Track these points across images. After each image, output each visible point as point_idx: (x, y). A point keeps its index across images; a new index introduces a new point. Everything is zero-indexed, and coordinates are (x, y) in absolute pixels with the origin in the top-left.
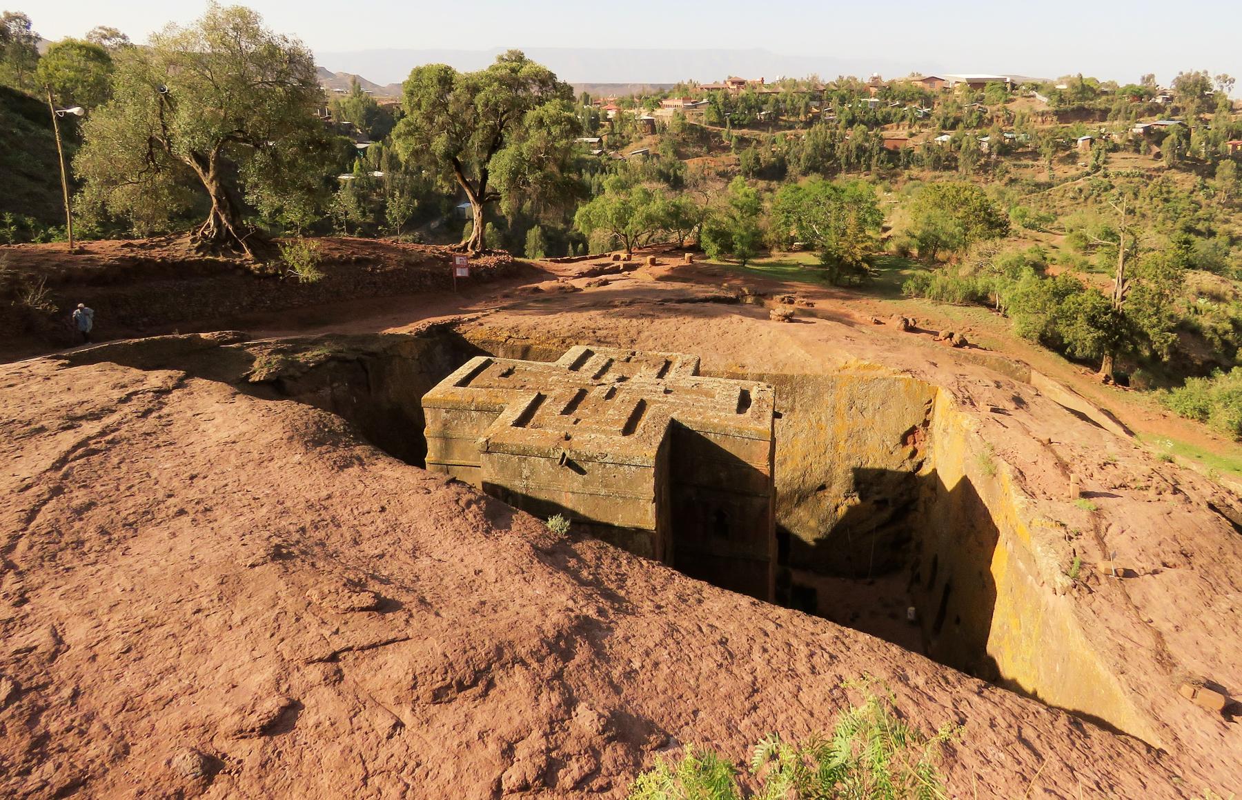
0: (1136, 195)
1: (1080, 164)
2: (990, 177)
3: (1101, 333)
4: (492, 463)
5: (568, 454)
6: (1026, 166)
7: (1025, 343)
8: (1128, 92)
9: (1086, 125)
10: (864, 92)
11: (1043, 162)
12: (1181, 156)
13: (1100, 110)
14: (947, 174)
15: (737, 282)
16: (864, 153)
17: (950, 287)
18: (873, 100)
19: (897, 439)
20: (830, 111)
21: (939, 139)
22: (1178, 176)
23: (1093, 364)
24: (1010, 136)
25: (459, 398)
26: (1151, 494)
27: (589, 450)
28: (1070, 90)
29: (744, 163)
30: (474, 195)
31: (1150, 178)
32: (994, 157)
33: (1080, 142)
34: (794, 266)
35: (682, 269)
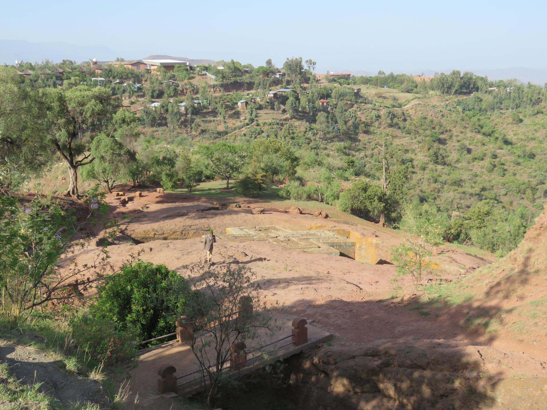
1: (242, 118)
2: (189, 130)
6: (210, 121)
8: (261, 71)
9: (240, 93)
11: (220, 118)
13: (247, 83)
18: (100, 79)
21: (153, 105)
22: (297, 123)
31: (282, 125)
32: (189, 116)
33: (239, 104)
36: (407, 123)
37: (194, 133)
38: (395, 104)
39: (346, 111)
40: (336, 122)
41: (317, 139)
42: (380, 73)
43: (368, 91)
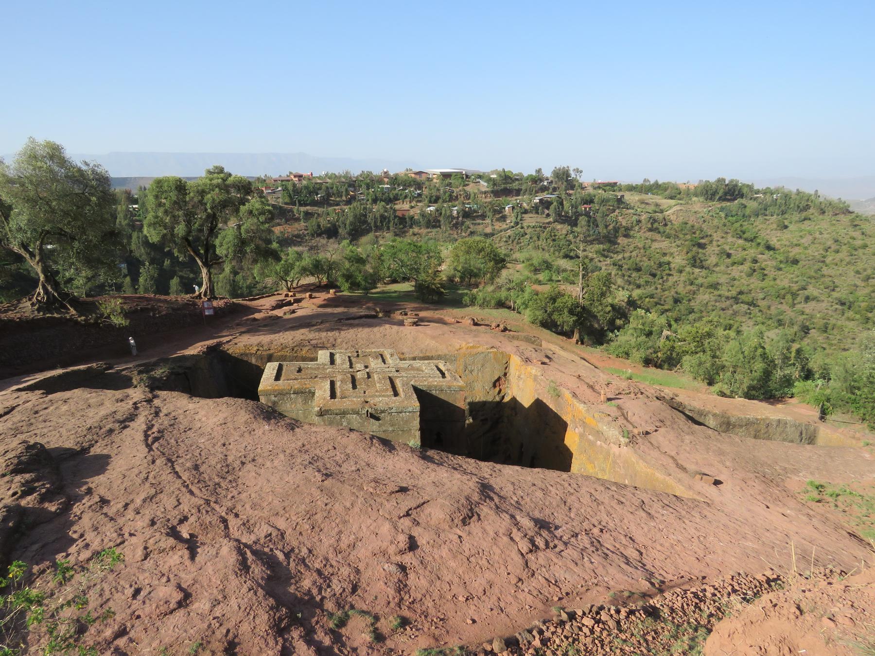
0: (538, 238)
1: (508, 221)
3: (575, 318)
4: (324, 421)
5: (370, 410)
6: (479, 224)
7: (534, 326)
9: (509, 199)
10: (380, 181)
11: (488, 221)
12: (560, 215)
14: (435, 230)
15: (370, 305)
16: (385, 219)
17: (488, 299)
18: (386, 186)
19: (491, 385)
20: (361, 194)
21: (429, 209)
22: (559, 226)
23: (568, 335)
24: (468, 206)
25: (283, 388)
26: (632, 395)
27: (381, 406)
28: (499, 178)
29: (310, 228)
30: (202, 262)
31: (545, 228)
32: (460, 219)
33: (507, 208)
34: (393, 292)
35: (329, 300)
36: (667, 227)
37: (464, 234)
38: (657, 210)
39: (607, 215)
40: (597, 226)
41: (578, 241)
42: (645, 180)
43: (632, 198)
